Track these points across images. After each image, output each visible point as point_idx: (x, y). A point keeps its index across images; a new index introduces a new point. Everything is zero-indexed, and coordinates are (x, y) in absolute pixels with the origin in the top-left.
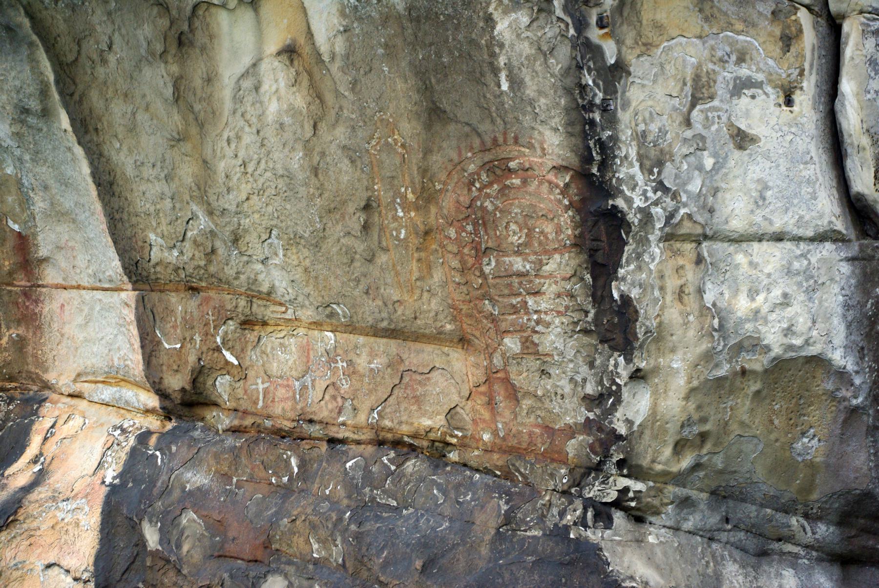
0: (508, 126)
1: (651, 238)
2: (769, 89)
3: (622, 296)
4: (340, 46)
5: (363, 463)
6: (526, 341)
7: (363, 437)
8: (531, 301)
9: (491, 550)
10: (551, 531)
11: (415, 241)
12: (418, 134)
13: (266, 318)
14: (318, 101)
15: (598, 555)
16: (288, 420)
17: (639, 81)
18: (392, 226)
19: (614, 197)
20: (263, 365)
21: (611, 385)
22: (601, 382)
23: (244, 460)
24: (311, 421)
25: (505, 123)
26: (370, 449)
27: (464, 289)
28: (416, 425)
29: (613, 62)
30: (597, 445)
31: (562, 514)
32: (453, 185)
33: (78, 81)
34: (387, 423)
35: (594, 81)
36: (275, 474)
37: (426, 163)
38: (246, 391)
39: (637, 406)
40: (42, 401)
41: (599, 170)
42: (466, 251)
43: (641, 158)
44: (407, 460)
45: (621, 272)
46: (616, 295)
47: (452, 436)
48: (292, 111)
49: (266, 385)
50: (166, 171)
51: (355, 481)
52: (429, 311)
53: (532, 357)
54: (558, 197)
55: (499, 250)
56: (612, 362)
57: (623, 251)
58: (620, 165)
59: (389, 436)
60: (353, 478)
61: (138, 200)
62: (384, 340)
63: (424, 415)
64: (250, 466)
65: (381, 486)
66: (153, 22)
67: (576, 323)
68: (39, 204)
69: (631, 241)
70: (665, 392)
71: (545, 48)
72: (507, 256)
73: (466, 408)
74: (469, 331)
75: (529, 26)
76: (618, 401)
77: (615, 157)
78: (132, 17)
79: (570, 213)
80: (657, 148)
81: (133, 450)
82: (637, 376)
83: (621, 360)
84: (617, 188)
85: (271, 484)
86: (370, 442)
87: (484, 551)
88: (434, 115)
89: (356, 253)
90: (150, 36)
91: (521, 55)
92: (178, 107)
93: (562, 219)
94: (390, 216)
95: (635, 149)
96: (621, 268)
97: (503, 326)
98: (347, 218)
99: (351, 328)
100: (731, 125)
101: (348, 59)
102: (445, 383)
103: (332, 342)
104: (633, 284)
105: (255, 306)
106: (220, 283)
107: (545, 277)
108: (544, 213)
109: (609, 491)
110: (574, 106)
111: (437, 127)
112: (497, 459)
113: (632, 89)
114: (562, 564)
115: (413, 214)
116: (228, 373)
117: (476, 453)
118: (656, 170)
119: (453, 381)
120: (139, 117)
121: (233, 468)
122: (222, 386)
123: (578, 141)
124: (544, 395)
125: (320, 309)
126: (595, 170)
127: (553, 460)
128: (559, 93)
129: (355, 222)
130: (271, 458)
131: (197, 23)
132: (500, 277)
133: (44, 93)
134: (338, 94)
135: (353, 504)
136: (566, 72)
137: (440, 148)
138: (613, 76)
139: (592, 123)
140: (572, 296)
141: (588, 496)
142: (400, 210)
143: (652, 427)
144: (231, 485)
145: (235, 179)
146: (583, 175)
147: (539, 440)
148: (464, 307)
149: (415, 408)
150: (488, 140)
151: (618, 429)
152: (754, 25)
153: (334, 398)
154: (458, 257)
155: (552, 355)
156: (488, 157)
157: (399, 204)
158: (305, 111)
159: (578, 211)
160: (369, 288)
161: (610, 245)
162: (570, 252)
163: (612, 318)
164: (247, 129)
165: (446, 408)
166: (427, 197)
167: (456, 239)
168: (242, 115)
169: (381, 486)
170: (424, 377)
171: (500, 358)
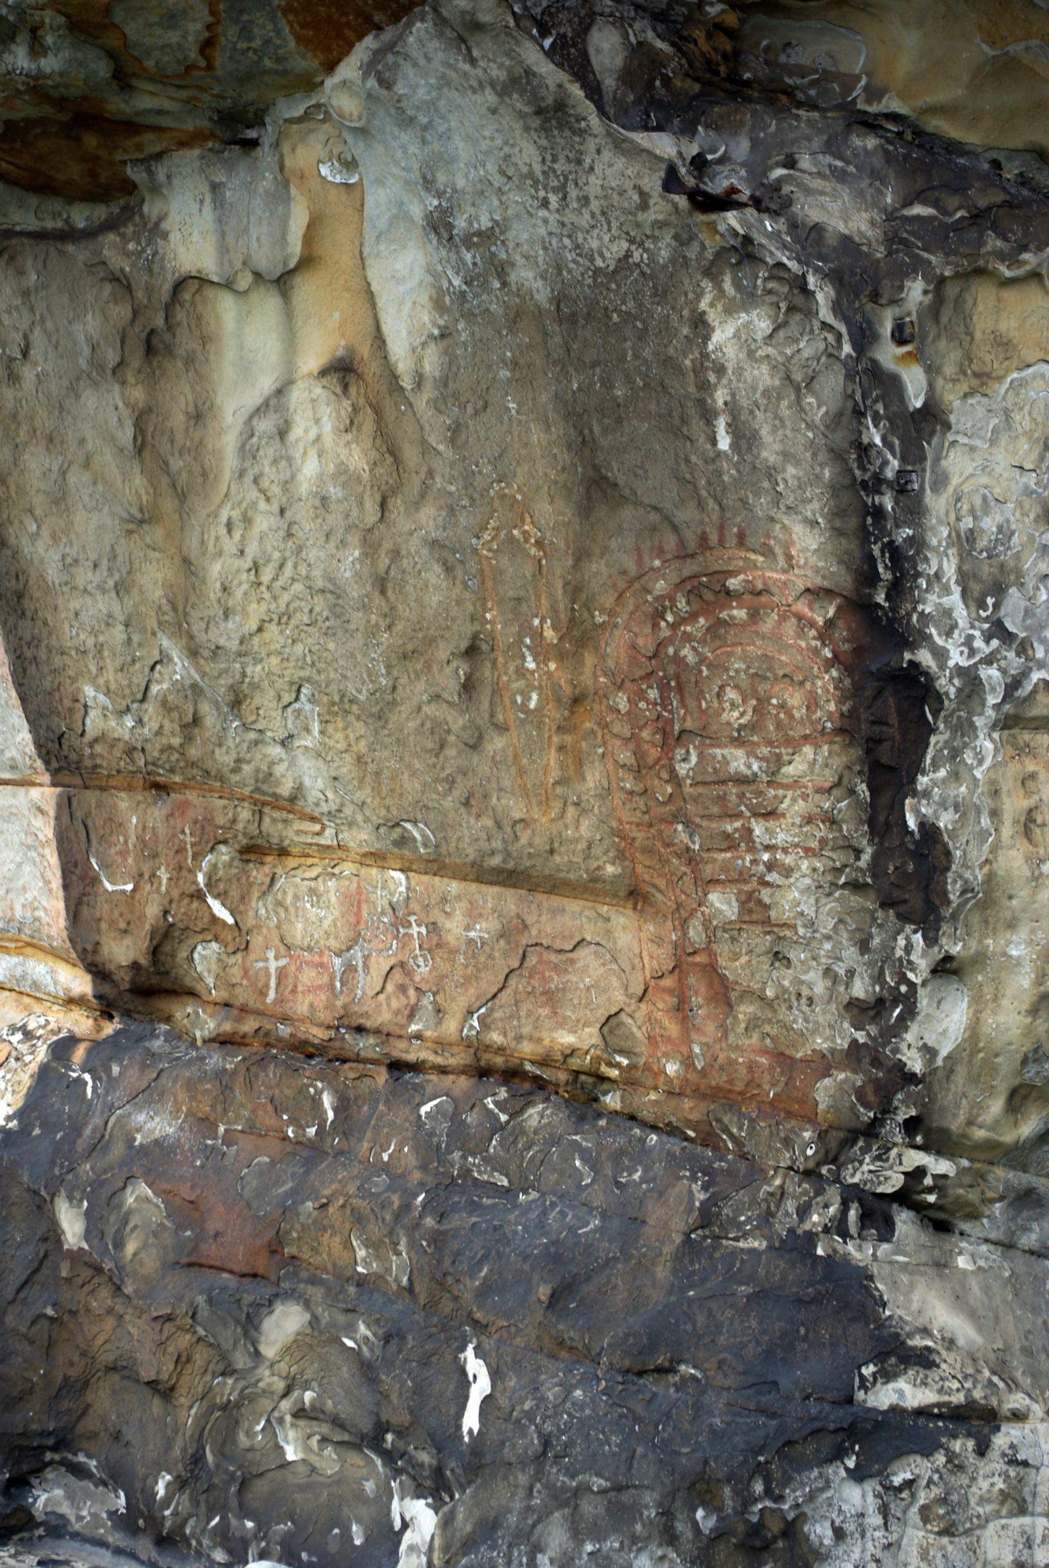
0: (728, 515)
1: (979, 721)
3: (922, 825)
4: (432, 363)
5: (450, 1108)
7: (452, 1061)
8: (758, 829)
9: (675, 1272)
10: (782, 1241)
11: (554, 714)
13: (287, 842)
14: (390, 460)
15: (867, 1288)
16: (319, 1025)
17: (966, 440)
19: (913, 647)
20: (278, 927)
21: (898, 983)
23: (239, 1095)
24: (360, 1029)
26: (463, 1083)
27: (641, 802)
28: (547, 1042)
29: (919, 404)
30: (870, 1091)
31: (803, 1212)
32: (626, 616)
34: (496, 1037)
35: (884, 439)
36: (292, 1121)
37: (579, 576)
38: (246, 972)
39: (944, 1023)
41: (888, 598)
42: (645, 734)
43: (963, 578)
45: (923, 781)
46: (912, 823)
47: (610, 1065)
48: (343, 475)
49: (282, 962)
50: (117, 576)
51: (435, 1140)
52: (577, 840)
53: (758, 929)
54: (814, 643)
55: (705, 735)
56: (901, 942)
57: (928, 745)
58: (927, 590)
59: (499, 1061)
61: (67, 627)
62: (495, 889)
63: (561, 1025)
64: (249, 1106)
65: (479, 1149)
66: (103, 310)
67: (838, 871)
70: (996, 999)
71: (798, 377)
72: (719, 747)
73: (637, 1015)
74: (646, 877)
75: (771, 336)
76: (910, 1012)
77: (918, 575)
78: (66, 300)
79: (835, 673)
80: (994, 561)
81: (44, 1070)
82: (946, 968)
83: (918, 938)
85: (285, 1138)
86: (464, 1071)
88: (596, 490)
89: (449, 732)
90: (96, 336)
91: (754, 389)
93: (819, 683)
94: (512, 669)
97: (708, 871)
98: (435, 668)
99: (436, 865)
101: (446, 385)
103: (403, 889)
104: (943, 805)
105: (267, 820)
106: (207, 778)
107: (786, 787)
108: (787, 671)
109: (888, 1173)
110: (847, 481)
112: (689, 1108)
113: (952, 455)
114: (800, 1301)
115: (552, 666)
116: (216, 939)
117: (653, 1096)
118: (990, 601)
119: (614, 966)
120: (72, 479)
121: (219, 1108)
122: (205, 959)
124: (777, 997)
125: (382, 830)
126: (880, 598)
127: (790, 1115)
128: (820, 458)
129: (450, 677)
130: (287, 1092)
131: (180, 315)
134: (426, 449)
135: (431, 1181)
136: (835, 421)
137: (605, 550)
138: (919, 431)
139: (878, 512)
140: (832, 822)
141: (850, 1181)
142: (529, 659)
143: (970, 1061)
144: (215, 1138)
145: (239, 594)
146: (858, 606)
147: (767, 1077)
148: (640, 836)
149: (545, 1012)
150: (691, 538)
151: (909, 1063)
153: (402, 989)
154: (631, 746)
155: (794, 927)
156: (690, 568)
157: (528, 648)
158: (366, 476)
159: (849, 670)
162: (832, 743)
163: (905, 863)
164: (262, 505)
165: (602, 1014)
166: (579, 637)
167: (629, 713)
168: (256, 481)
169: (479, 1149)
170: (563, 957)
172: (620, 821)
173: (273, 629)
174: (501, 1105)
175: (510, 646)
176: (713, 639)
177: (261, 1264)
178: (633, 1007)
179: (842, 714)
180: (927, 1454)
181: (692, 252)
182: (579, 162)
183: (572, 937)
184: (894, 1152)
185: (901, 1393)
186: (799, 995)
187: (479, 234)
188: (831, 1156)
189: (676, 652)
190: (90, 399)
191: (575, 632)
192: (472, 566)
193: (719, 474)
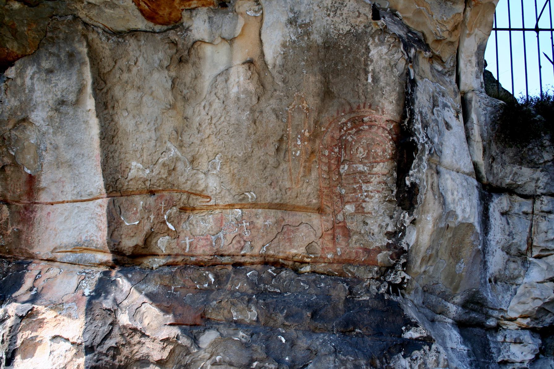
1: (424, 158)
2: (452, 109)
5: (257, 273)
6: (359, 206)
8: (364, 187)
9: (345, 307)
14: (261, 87)
16: (208, 255)
19: (413, 136)
20: (190, 230)
22: (396, 226)
23: (178, 278)
24: (222, 256)
25: (366, 98)
26: (259, 267)
31: (378, 288)
33: (108, 82)
34: (271, 252)
36: (199, 283)
38: (178, 244)
39: (411, 238)
40: (29, 264)
42: (332, 162)
43: (422, 122)
45: (411, 172)
46: (408, 183)
47: (308, 258)
50: (156, 126)
52: (306, 193)
55: (350, 161)
56: (402, 215)
57: (412, 163)
59: (272, 259)
60: (253, 280)
61: (131, 143)
62: (274, 210)
63: (293, 247)
65: (269, 283)
66: (165, 51)
67: (386, 197)
68: (48, 158)
70: (423, 232)
74: (325, 203)
76: (404, 234)
77: (414, 118)
78: (152, 49)
79: (391, 143)
81: (100, 280)
85: (196, 288)
87: (341, 306)
88: (327, 94)
91: (381, 66)
92: (172, 92)
94: (293, 144)
97: (346, 199)
98: (268, 145)
99: (254, 205)
100: (444, 119)
101: (283, 67)
102: (307, 231)
104: (416, 178)
105: (191, 199)
106: (172, 187)
107: (374, 174)
110: (402, 92)
114: (383, 311)
115: (306, 143)
116: (168, 235)
117: (323, 265)
119: (312, 229)
120: (144, 99)
121: (172, 282)
123: (401, 108)
125: (236, 197)
126: (406, 123)
130: (196, 275)
131: (193, 51)
133: (81, 91)
135: (256, 292)
136: (400, 76)
137: (327, 110)
140: (385, 183)
145: (204, 126)
146: (399, 125)
147: (362, 255)
148: (325, 191)
149: (288, 244)
152: (445, 84)
154: (328, 165)
155: (371, 213)
156: (352, 115)
157: (299, 138)
158: (253, 92)
160: (273, 182)
164: (217, 100)
166: (315, 136)
167: (328, 156)
168: (215, 94)
169: (269, 283)
173: (213, 137)
174: (273, 271)
175: (293, 138)
177: (198, 321)
180: (419, 350)
181: (368, 30)
182: (342, 4)
187: (305, 24)
190: (156, 75)
193: (367, 89)
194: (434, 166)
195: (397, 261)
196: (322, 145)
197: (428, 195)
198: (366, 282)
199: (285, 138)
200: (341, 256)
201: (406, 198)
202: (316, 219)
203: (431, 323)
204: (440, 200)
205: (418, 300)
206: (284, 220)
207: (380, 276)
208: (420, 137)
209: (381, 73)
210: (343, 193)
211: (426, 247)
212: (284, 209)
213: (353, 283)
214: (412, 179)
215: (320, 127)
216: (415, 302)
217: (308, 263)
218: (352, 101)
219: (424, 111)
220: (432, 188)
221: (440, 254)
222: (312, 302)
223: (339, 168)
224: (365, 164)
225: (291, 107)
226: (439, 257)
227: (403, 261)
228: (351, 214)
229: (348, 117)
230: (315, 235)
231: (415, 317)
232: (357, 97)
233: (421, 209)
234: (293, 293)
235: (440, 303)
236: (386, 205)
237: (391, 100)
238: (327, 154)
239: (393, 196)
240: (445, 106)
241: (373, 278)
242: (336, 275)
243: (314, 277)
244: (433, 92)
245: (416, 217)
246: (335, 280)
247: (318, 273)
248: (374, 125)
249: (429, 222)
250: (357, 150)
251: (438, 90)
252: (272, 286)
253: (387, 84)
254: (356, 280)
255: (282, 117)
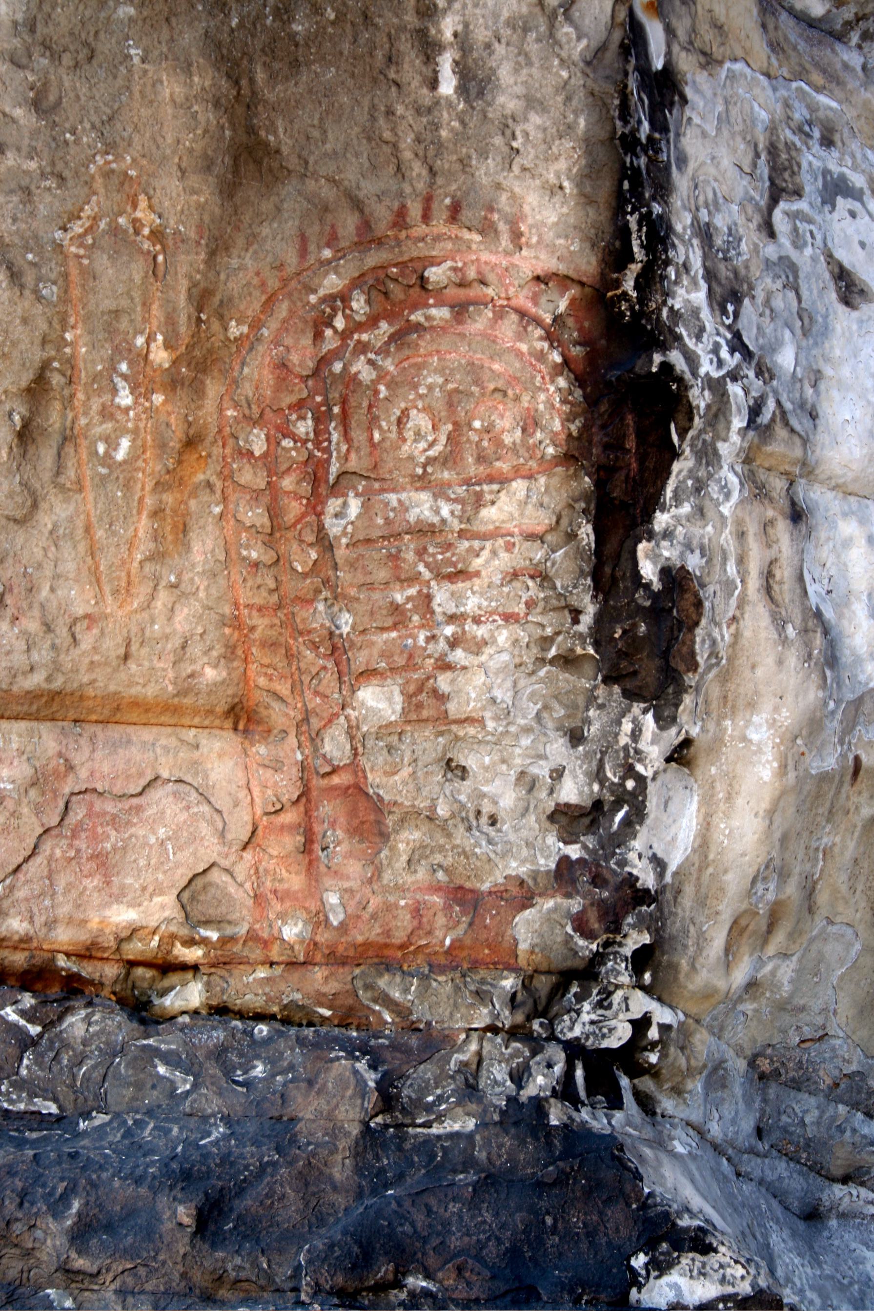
0: (440, 181)
1: (723, 448)
3: (666, 572)
6: (420, 690)
9: (358, 1170)
10: (503, 1113)
11: (153, 466)
12: (200, 207)
15: (620, 1160)
18: (98, 430)
19: (664, 348)
21: (623, 779)
31: (519, 1077)
37: (211, 275)
41: (636, 287)
42: (288, 483)
43: (710, 275)
44: (68, 1011)
45: (661, 520)
46: (648, 570)
47: (190, 942)
52: (167, 637)
56: (627, 726)
57: (669, 473)
58: (676, 283)
59: (18, 959)
62: (23, 725)
63: (118, 897)
67: (546, 642)
69: (688, 451)
70: (729, 798)
72: (394, 490)
74: (262, 681)
76: (638, 814)
77: (667, 262)
79: (562, 382)
83: (649, 719)
84: (671, 331)
87: (341, 1169)
88: (246, 160)
91: (496, 16)
94: (95, 405)
95: (699, 253)
96: (662, 511)
97: (360, 660)
100: (829, 256)
101: (32, 30)
102: (183, 817)
104: (688, 547)
107: (484, 537)
108: (500, 384)
109: (613, 1023)
110: (604, 135)
111: (250, 190)
112: (320, 979)
114: (539, 1186)
115: (158, 399)
117: (262, 973)
118: (730, 308)
119: (205, 808)
123: (601, 215)
124: (453, 816)
126: (629, 285)
128: (574, 102)
132: (368, 541)
136: (593, 60)
140: (542, 577)
141: (570, 1035)
143: (698, 879)
146: (599, 298)
148: (261, 623)
151: (642, 876)
152: (839, 83)
154: (266, 499)
155: (481, 722)
156: (373, 259)
157: (124, 377)
159: (580, 380)
161: (642, 459)
163: (635, 626)
165: (181, 877)
166: (198, 363)
167: (265, 455)
170: (126, 804)
171: (343, 739)
172: (236, 605)
174: (29, 1015)
176: (399, 349)
178: (233, 858)
179: (570, 435)
183: (141, 774)
184: (617, 997)
185: (676, 1287)
186: (479, 813)
188: (540, 1008)
189: (345, 368)
191: (197, 353)
192: (51, 269)
193: (436, 127)
194: (778, 485)
195: (607, 944)
196: (236, 405)
197: (748, 626)
198: (460, 1050)
199: (56, 380)
200: (343, 927)
201: (643, 641)
202: (220, 760)
203: (801, 1225)
204: (808, 645)
205: (732, 1118)
206: (70, 768)
207: (529, 1018)
208: (701, 350)
209: (500, 49)
210: (346, 630)
211: (751, 872)
212: (72, 714)
213: (397, 1057)
214: (668, 552)
215: (221, 317)
216: (715, 1130)
217: (195, 968)
218: (368, 188)
219: (720, 222)
220: (768, 590)
221: (823, 898)
222: (206, 1156)
223: (319, 515)
224: (440, 491)
225: (77, 228)
226: (823, 911)
227: (635, 939)
228: (385, 730)
229: (350, 268)
230: (222, 834)
231: (697, 1202)
232: (392, 169)
233: (715, 692)
234: (117, 1115)
235: (841, 1130)
236: (549, 680)
237: (552, 178)
238: (259, 446)
239: (581, 636)
240: (835, 189)
241: (493, 1029)
242: (324, 1020)
243: (219, 1035)
244: (772, 129)
245: (695, 731)
246: (316, 1045)
247: (241, 1015)
248: (475, 303)
249: (760, 751)
250: (400, 422)
251: (800, 114)
252: (20, 1085)
253: (532, 102)
254: (414, 1041)
255: (39, 279)
